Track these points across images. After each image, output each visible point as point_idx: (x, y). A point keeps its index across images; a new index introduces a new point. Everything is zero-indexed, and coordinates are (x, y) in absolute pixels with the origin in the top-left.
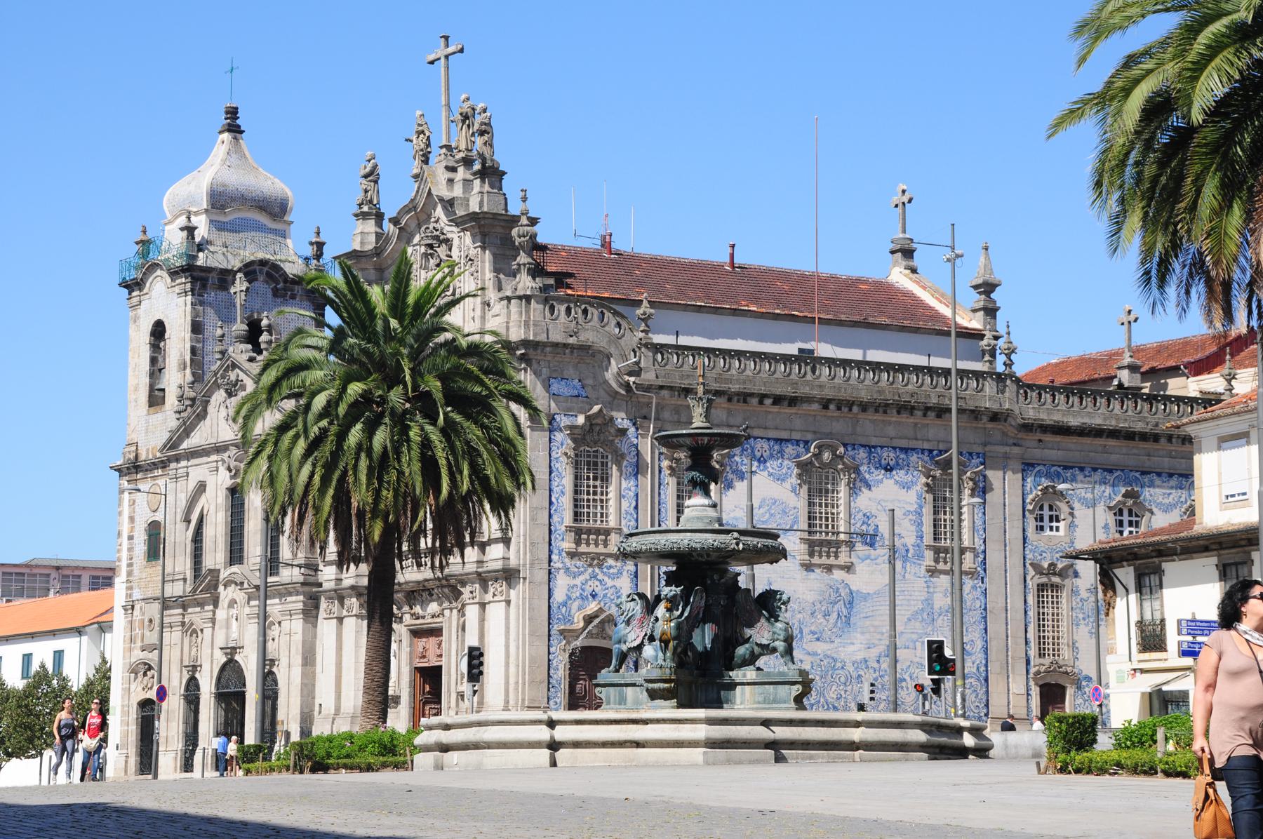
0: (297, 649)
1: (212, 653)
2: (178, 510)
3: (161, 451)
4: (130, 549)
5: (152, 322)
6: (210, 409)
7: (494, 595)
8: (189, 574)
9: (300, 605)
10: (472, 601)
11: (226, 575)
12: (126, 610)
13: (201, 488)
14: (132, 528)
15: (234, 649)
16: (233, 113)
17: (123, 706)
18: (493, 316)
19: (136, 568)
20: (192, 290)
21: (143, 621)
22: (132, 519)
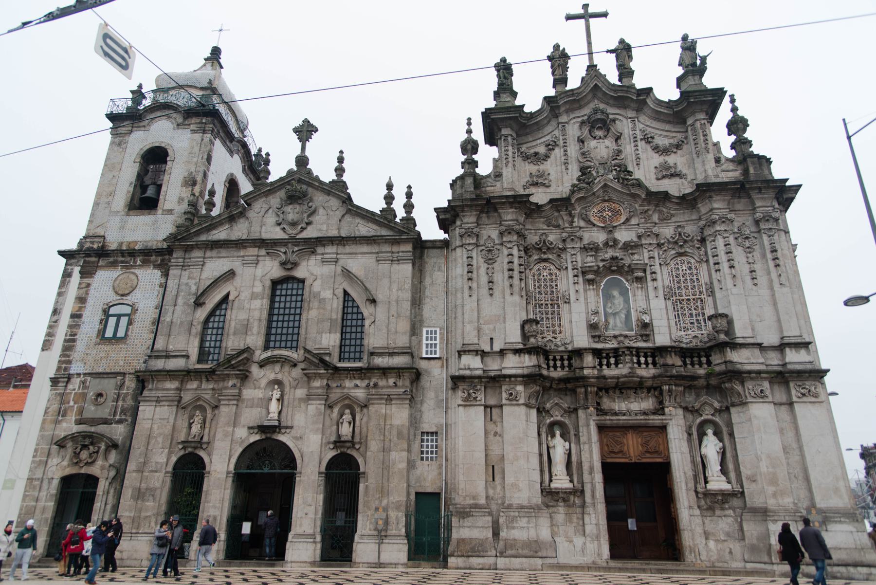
0: (400, 435)
1: (233, 431)
3: (164, 240)
5: (151, 146)
7: (804, 395)
8: (194, 352)
10: (761, 400)
12: (55, 381)
13: (230, 274)
14: (80, 309)
16: (216, 53)
17: (30, 480)
18: (723, 171)
19: (80, 346)
20: (212, 131)
21: (84, 396)
22: (82, 300)
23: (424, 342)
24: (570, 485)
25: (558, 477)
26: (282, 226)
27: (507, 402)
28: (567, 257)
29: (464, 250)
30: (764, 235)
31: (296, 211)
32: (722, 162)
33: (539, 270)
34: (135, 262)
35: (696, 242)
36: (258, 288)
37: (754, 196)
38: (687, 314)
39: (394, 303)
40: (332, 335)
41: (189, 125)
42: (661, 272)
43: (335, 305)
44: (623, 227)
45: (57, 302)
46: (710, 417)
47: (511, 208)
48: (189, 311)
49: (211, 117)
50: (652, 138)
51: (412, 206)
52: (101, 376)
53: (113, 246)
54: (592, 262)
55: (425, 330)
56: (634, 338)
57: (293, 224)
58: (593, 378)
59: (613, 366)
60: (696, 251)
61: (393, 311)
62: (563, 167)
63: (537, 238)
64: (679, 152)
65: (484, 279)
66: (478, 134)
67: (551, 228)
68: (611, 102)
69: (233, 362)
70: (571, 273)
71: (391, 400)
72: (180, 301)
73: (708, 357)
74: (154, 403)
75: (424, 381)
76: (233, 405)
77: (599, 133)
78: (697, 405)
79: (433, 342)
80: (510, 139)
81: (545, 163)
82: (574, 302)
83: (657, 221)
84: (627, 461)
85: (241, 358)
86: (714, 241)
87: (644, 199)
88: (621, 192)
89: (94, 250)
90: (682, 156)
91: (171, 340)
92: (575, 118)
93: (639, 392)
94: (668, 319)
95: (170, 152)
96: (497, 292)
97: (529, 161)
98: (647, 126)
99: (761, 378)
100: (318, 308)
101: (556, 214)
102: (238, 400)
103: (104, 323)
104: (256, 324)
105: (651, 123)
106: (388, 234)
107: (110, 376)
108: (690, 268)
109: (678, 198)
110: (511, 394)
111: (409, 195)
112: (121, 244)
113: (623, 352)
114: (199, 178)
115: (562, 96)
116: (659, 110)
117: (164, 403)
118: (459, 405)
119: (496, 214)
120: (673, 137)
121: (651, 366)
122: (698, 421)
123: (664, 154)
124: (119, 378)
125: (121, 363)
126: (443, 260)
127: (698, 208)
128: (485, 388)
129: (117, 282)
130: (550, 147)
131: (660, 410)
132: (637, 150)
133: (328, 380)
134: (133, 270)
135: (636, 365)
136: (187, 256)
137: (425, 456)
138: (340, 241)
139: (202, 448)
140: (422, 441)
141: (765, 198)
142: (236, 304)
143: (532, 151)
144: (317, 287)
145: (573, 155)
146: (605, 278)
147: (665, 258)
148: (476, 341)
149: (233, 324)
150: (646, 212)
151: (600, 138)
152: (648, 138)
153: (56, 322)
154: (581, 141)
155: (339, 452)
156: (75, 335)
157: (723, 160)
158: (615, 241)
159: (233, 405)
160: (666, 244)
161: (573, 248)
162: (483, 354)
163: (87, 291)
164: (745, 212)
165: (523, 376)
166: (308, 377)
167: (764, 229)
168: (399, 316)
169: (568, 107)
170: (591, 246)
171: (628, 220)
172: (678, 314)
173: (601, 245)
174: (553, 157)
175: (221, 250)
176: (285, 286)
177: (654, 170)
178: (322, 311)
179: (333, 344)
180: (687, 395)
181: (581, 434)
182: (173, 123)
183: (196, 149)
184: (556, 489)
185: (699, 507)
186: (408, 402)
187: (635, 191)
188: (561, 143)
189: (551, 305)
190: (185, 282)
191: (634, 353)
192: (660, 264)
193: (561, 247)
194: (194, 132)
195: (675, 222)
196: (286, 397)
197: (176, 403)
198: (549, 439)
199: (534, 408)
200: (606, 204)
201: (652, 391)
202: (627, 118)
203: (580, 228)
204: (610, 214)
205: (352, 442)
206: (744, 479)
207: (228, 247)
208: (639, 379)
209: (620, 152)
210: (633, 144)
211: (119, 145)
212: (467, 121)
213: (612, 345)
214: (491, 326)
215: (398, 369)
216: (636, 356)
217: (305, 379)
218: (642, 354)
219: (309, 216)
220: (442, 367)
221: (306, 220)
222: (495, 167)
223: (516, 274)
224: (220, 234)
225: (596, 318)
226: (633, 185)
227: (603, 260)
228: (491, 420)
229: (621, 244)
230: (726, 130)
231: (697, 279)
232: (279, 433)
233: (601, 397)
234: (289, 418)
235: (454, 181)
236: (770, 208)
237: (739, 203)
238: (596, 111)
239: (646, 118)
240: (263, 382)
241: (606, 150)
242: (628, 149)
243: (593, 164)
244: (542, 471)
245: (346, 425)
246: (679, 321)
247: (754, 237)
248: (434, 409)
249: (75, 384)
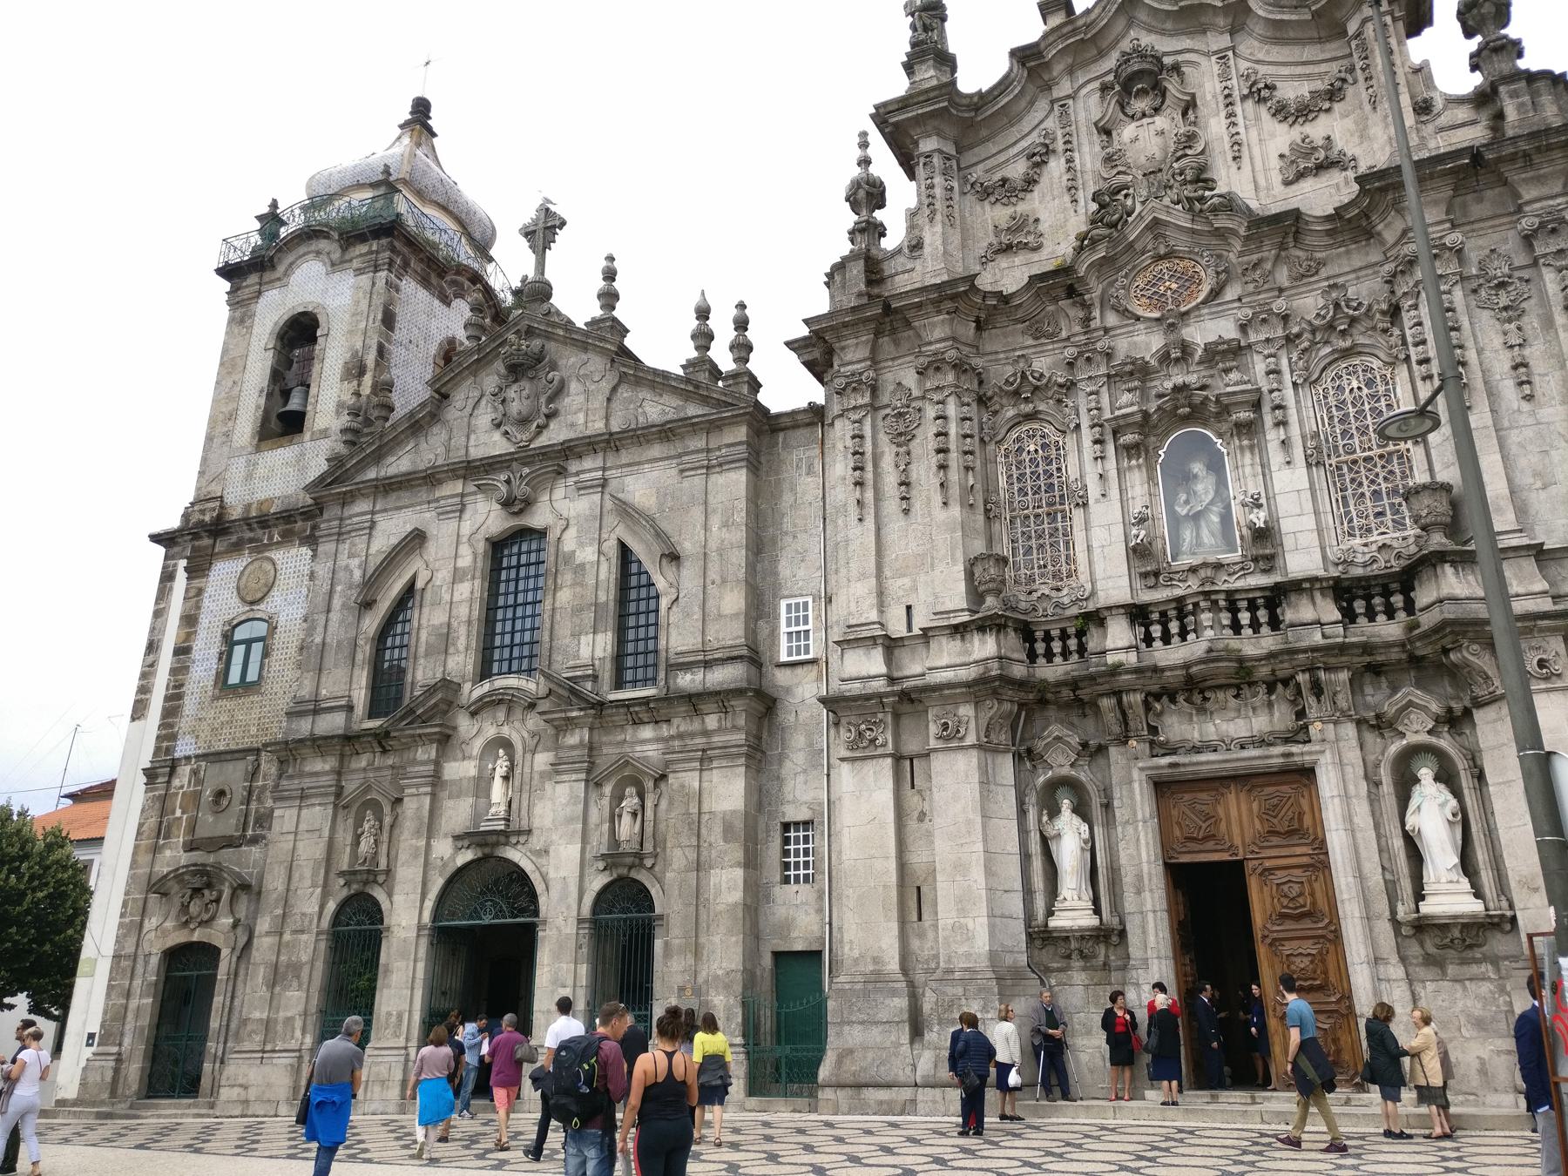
1: (428, 845)
2: (339, 588)
4: (180, 671)
5: (286, 318)
6: (453, 413)
8: (360, 697)
9: (740, 737)
11: (477, 693)
13: (416, 540)
14: (189, 636)
15: (505, 836)
18: (1442, 130)
23: (784, 628)
24: (1094, 921)
25: (1067, 904)
26: (503, 428)
27: (940, 745)
28: (1083, 402)
29: (847, 422)
30: (1544, 270)
31: (524, 393)
32: (1435, 112)
33: (1018, 439)
34: (271, 538)
35: (1378, 316)
36: (465, 561)
37: (1514, 176)
38: (1368, 494)
39: (713, 556)
40: (600, 637)
41: (351, 260)
42: (1298, 402)
43: (603, 575)
44: (1206, 311)
45: (152, 629)
46: (1423, 738)
47: (939, 312)
48: (351, 618)
49: (387, 236)
50: (1271, 87)
51: (749, 348)
52: (223, 757)
53: (236, 513)
54: (1132, 405)
55: (783, 604)
56: (1237, 567)
57: (523, 421)
58: (1128, 672)
59: (1176, 639)
60: (1381, 340)
61: (713, 574)
62: (1067, 198)
63: (1009, 370)
64: (1337, 107)
65: (891, 479)
66: (886, 165)
67: (1043, 340)
68: (1169, 25)
69: (419, 712)
70: (1087, 435)
71: (711, 759)
72: (337, 603)
74: (297, 802)
75: (786, 717)
76: (425, 794)
77: (1139, 105)
78: (1389, 709)
79: (802, 628)
80: (936, 160)
81: (1029, 196)
82: (1097, 501)
83: (1286, 284)
84: (1225, 857)
85: (433, 701)
87: (1247, 238)
88: (1193, 231)
89: (206, 525)
90: (1344, 116)
91: (323, 679)
92: (1089, 81)
93: (1246, 691)
94: (1316, 513)
95: (321, 319)
96: (917, 506)
97: (993, 199)
98: (1258, 62)
99: (1541, 630)
100: (572, 586)
101: (1051, 308)
102: (433, 785)
103: (226, 658)
104: (463, 630)
105: (1268, 52)
106: (700, 412)
107: (241, 755)
108: (1370, 383)
109: (1328, 218)
110: (945, 726)
111: (742, 324)
112: (248, 507)
113: (1196, 605)
115: (1051, 39)
116: (1279, 17)
117: (314, 801)
118: (842, 760)
119: (911, 333)
120: (1320, 75)
121: (1265, 630)
122: (1395, 747)
123: (1301, 120)
124: (251, 758)
125: (253, 730)
126: (818, 451)
127: (1379, 234)
128: (897, 716)
129: (244, 578)
130: (1037, 159)
131: (1299, 734)
132: (1234, 124)
133: (591, 729)
134: (267, 554)
136: (346, 514)
138: (609, 443)
139: (375, 882)
140: (786, 841)
141: (1545, 176)
142: (428, 596)
143: (997, 177)
144: (569, 543)
145: (1089, 165)
146: (1167, 435)
147: (1307, 369)
148: (873, 616)
149: (424, 635)
150: (1256, 266)
151: (1144, 115)
152: (1259, 90)
153: (152, 665)
154: (1106, 131)
155: (615, 876)
156: (182, 685)
157: (1439, 104)
158: (1186, 349)
159: (425, 794)
160: (1306, 335)
161: (1090, 378)
162: (891, 646)
163: (198, 602)
164: (1497, 222)
165: (968, 685)
166: (556, 727)
167: (1545, 256)
168: (724, 581)
169: (1070, 61)
170: (1128, 368)
171: (1216, 293)
172: (1344, 498)
173: (1153, 362)
174: (1044, 181)
175: (402, 493)
176: (515, 549)
177: (1275, 163)
178: (578, 589)
179: (601, 655)
180: (1368, 690)
181: (1116, 803)
182: (325, 264)
183: (364, 305)
184: (1056, 930)
185: (1403, 959)
186: (697, 764)
187: (1222, 222)
188: (1060, 145)
189: (1049, 514)
190: (344, 564)
191: (1222, 603)
192: (1295, 384)
193: (1061, 380)
195: (1328, 278)
196: (518, 771)
197: (332, 799)
198: (1045, 818)
199: (1006, 751)
200: (1165, 265)
201: (1280, 686)
202: (1207, 54)
203: (1106, 330)
204: (1174, 286)
205: (639, 856)
206: (1513, 884)
207: (413, 486)
208: (1235, 665)
209: (1191, 138)
210: (1223, 114)
212: (857, 140)
214: (906, 581)
215: (718, 693)
216: (1229, 610)
217: (551, 731)
218: (1244, 604)
219: (551, 400)
220: (819, 679)
221: (544, 410)
222: (912, 227)
223: (954, 458)
224: (400, 463)
225: (1143, 533)
226: (1215, 210)
227: (1160, 396)
228: (913, 787)
229: (1200, 352)
230: (1458, 25)
232: (507, 844)
233: (1160, 715)
234: (524, 812)
235: (830, 276)
236: (1559, 200)
237: (1480, 200)
238: (1141, 54)
239: (1256, 43)
240: (477, 745)
241: (1159, 140)
242: (1214, 127)
243: (1129, 178)
244: (1028, 892)
245: (626, 819)
246: (1347, 513)
247: (1520, 279)
248: (805, 771)
249: (185, 771)
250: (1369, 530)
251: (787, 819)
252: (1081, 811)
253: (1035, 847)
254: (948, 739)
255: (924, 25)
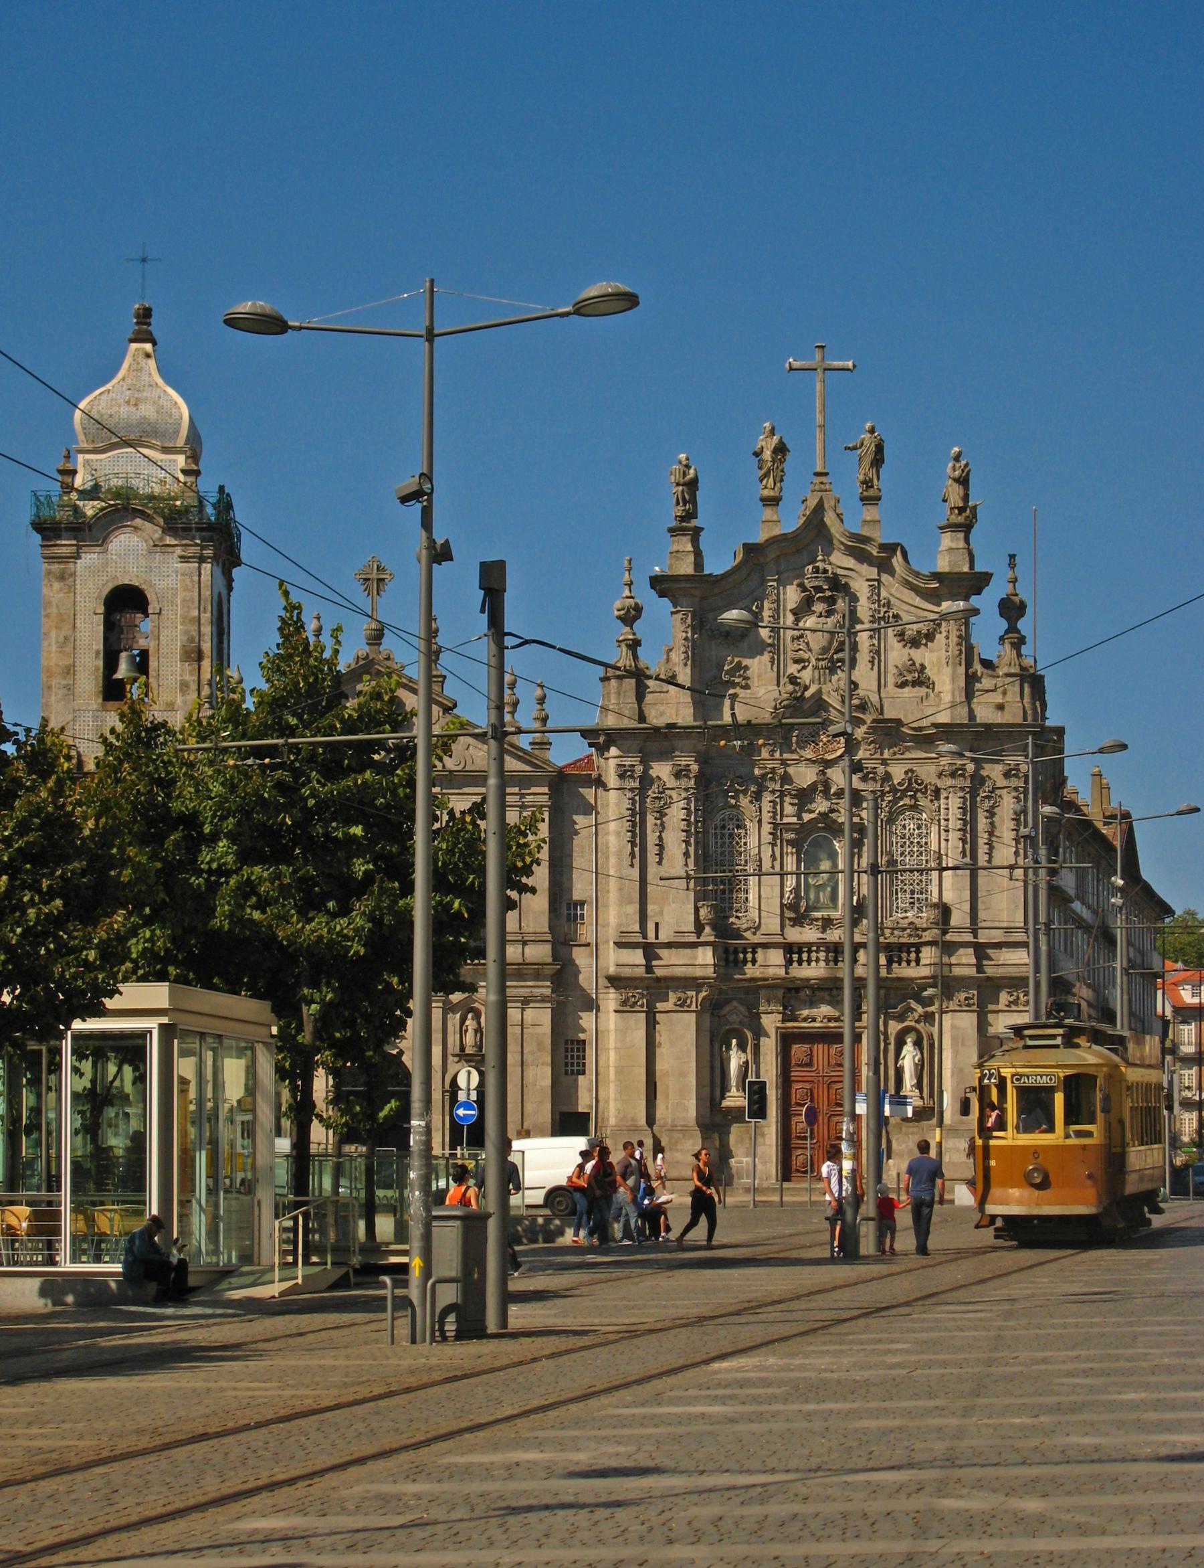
0: (540, 1045)
16: (145, 315)
33: (723, 820)
46: (913, 1024)
59: (805, 964)
73: (918, 952)
86: (947, 798)
95: (151, 596)
105: (897, 589)
108: (919, 827)
114: (207, 647)
135: (832, 964)
137: (569, 1068)
177: (892, 670)
194: (185, 559)
211: (62, 577)
213: (809, 934)
231: (926, 843)
250: (906, 911)
251: (570, 1038)
252: (742, 1047)
253: (717, 1064)
254: (680, 1006)
255: (684, 498)
